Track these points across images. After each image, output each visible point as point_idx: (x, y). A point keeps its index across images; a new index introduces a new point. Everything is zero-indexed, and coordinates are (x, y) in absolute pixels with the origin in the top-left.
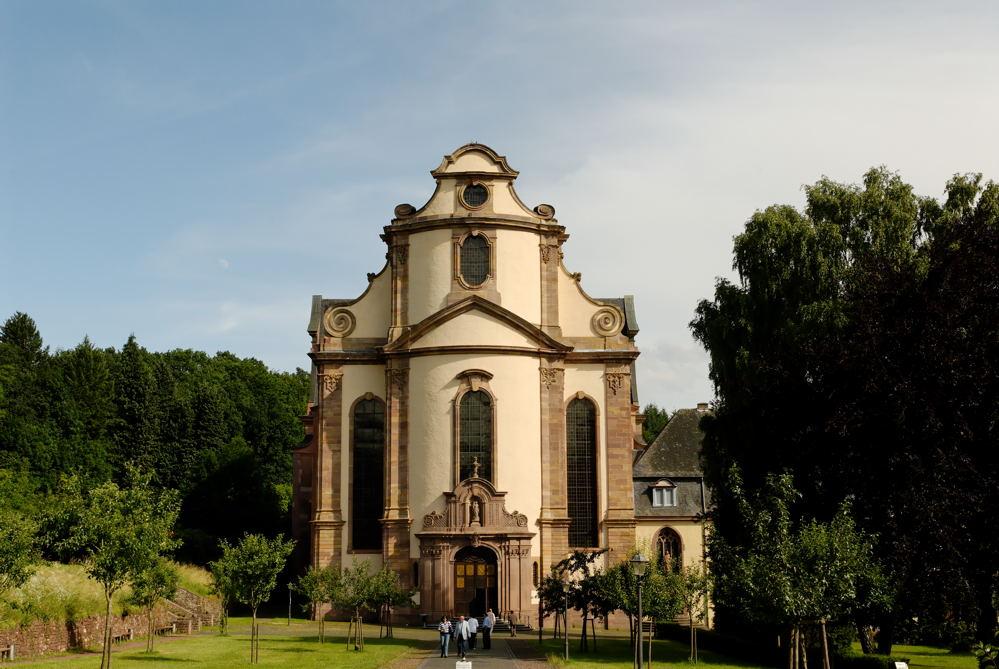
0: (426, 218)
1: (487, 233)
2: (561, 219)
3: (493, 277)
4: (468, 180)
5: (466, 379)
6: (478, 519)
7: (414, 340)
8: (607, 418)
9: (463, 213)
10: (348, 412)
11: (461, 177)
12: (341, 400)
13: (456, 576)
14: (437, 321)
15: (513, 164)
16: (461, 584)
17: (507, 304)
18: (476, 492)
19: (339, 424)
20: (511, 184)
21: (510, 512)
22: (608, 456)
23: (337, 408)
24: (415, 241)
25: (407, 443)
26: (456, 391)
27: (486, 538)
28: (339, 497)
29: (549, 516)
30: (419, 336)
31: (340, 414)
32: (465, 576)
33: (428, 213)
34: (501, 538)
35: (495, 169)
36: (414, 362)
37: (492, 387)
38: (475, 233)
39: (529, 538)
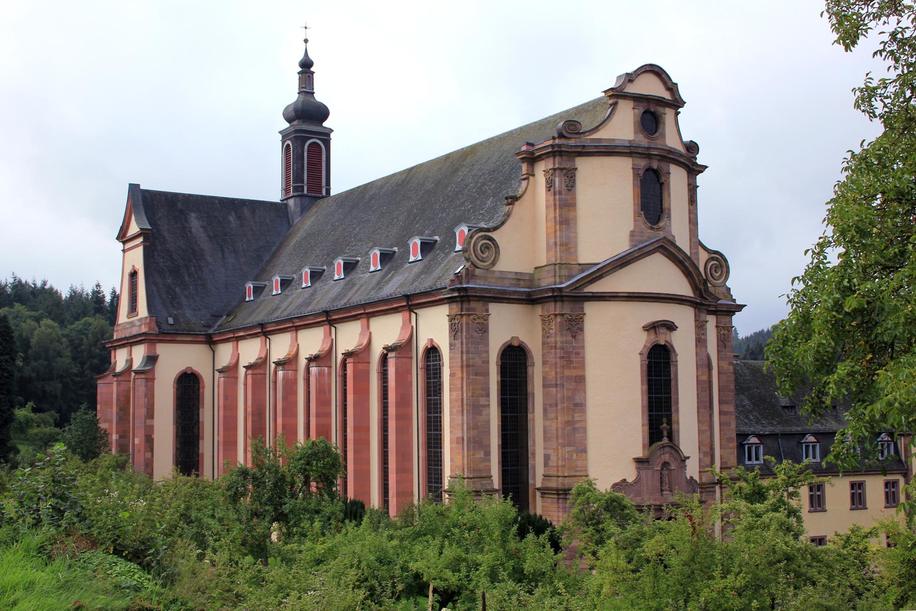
0: (600, 140)
2: (700, 160)
3: (669, 217)
4: (645, 104)
5: (652, 331)
7: (592, 281)
9: (643, 141)
10: (495, 360)
11: (638, 99)
12: (487, 344)
14: (622, 262)
15: (683, 93)
19: (487, 374)
20: (677, 114)
23: (484, 355)
24: (586, 167)
25: (585, 398)
26: (641, 341)
28: (490, 461)
30: (600, 277)
31: (488, 362)
33: (601, 135)
35: (667, 96)
36: (591, 310)
38: (655, 165)
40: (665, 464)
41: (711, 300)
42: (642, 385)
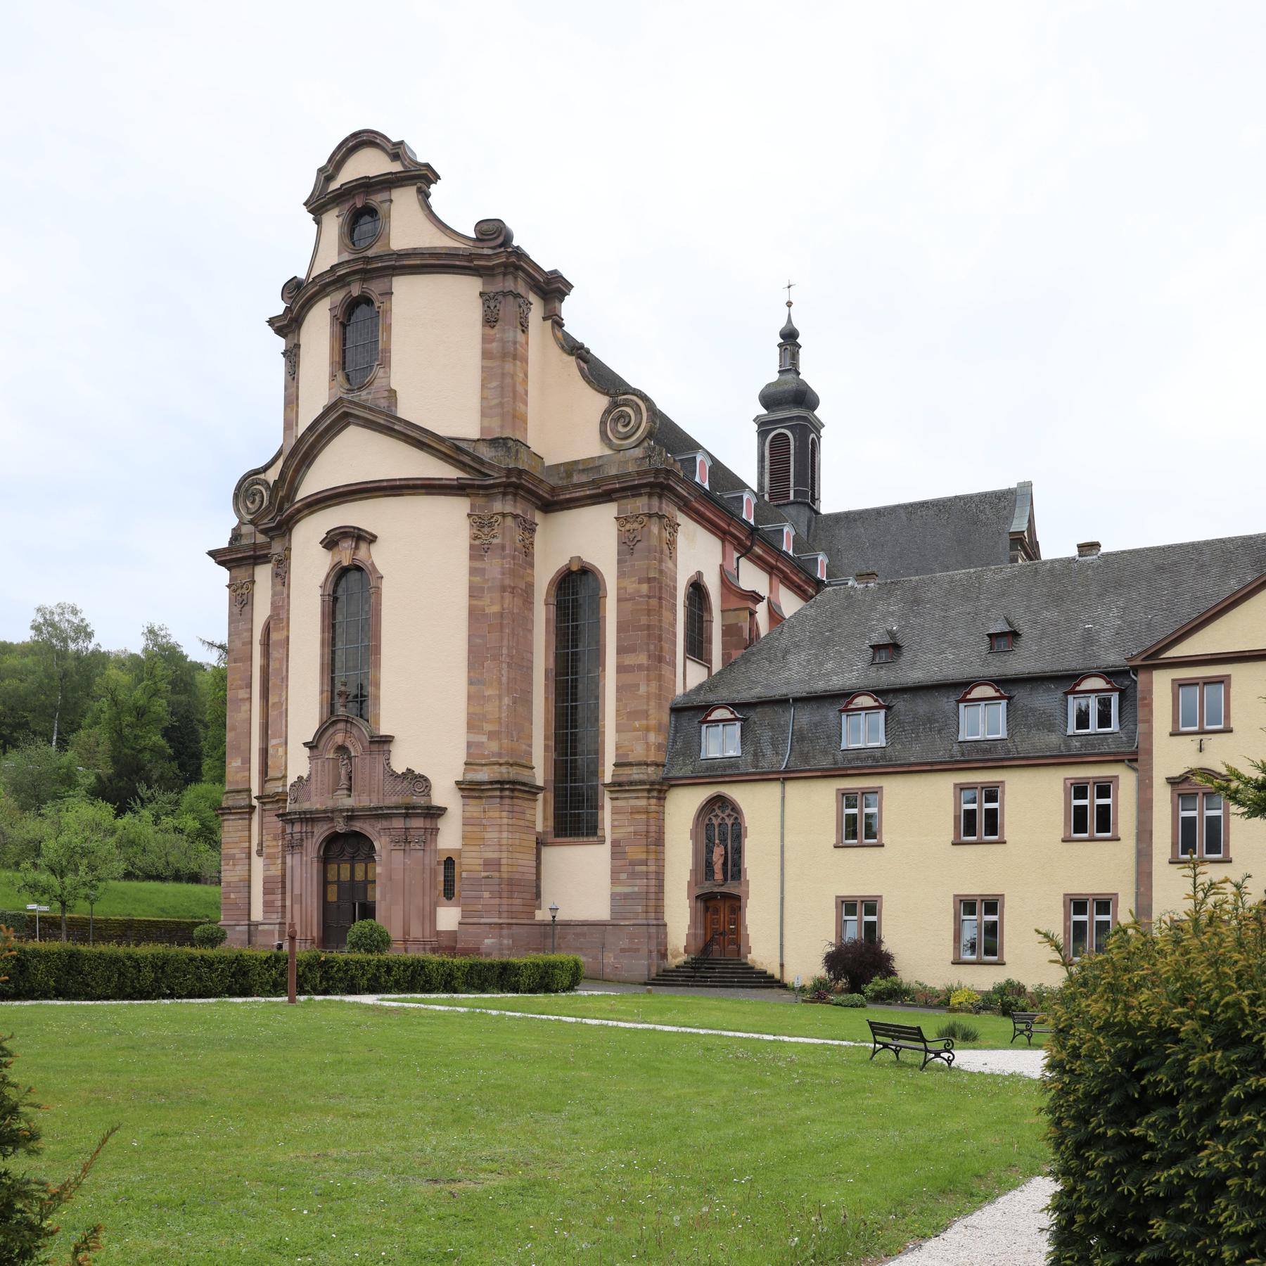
1: (375, 288)
3: (386, 363)
6: (344, 781)
8: (619, 600)
13: (325, 883)
16: (333, 896)
17: (408, 410)
18: (339, 738)
20: (424, 195)
21: (399, 768)
22: (621, 669)
27: (352, 815)
29: (483, 775)
32: (338, 882)
34: (377, 814)
37: (380, 557)
38: (356, 290)
39: (440, 816)
40: (342, 749)
41: (496, 475)
42: (323, 631)
